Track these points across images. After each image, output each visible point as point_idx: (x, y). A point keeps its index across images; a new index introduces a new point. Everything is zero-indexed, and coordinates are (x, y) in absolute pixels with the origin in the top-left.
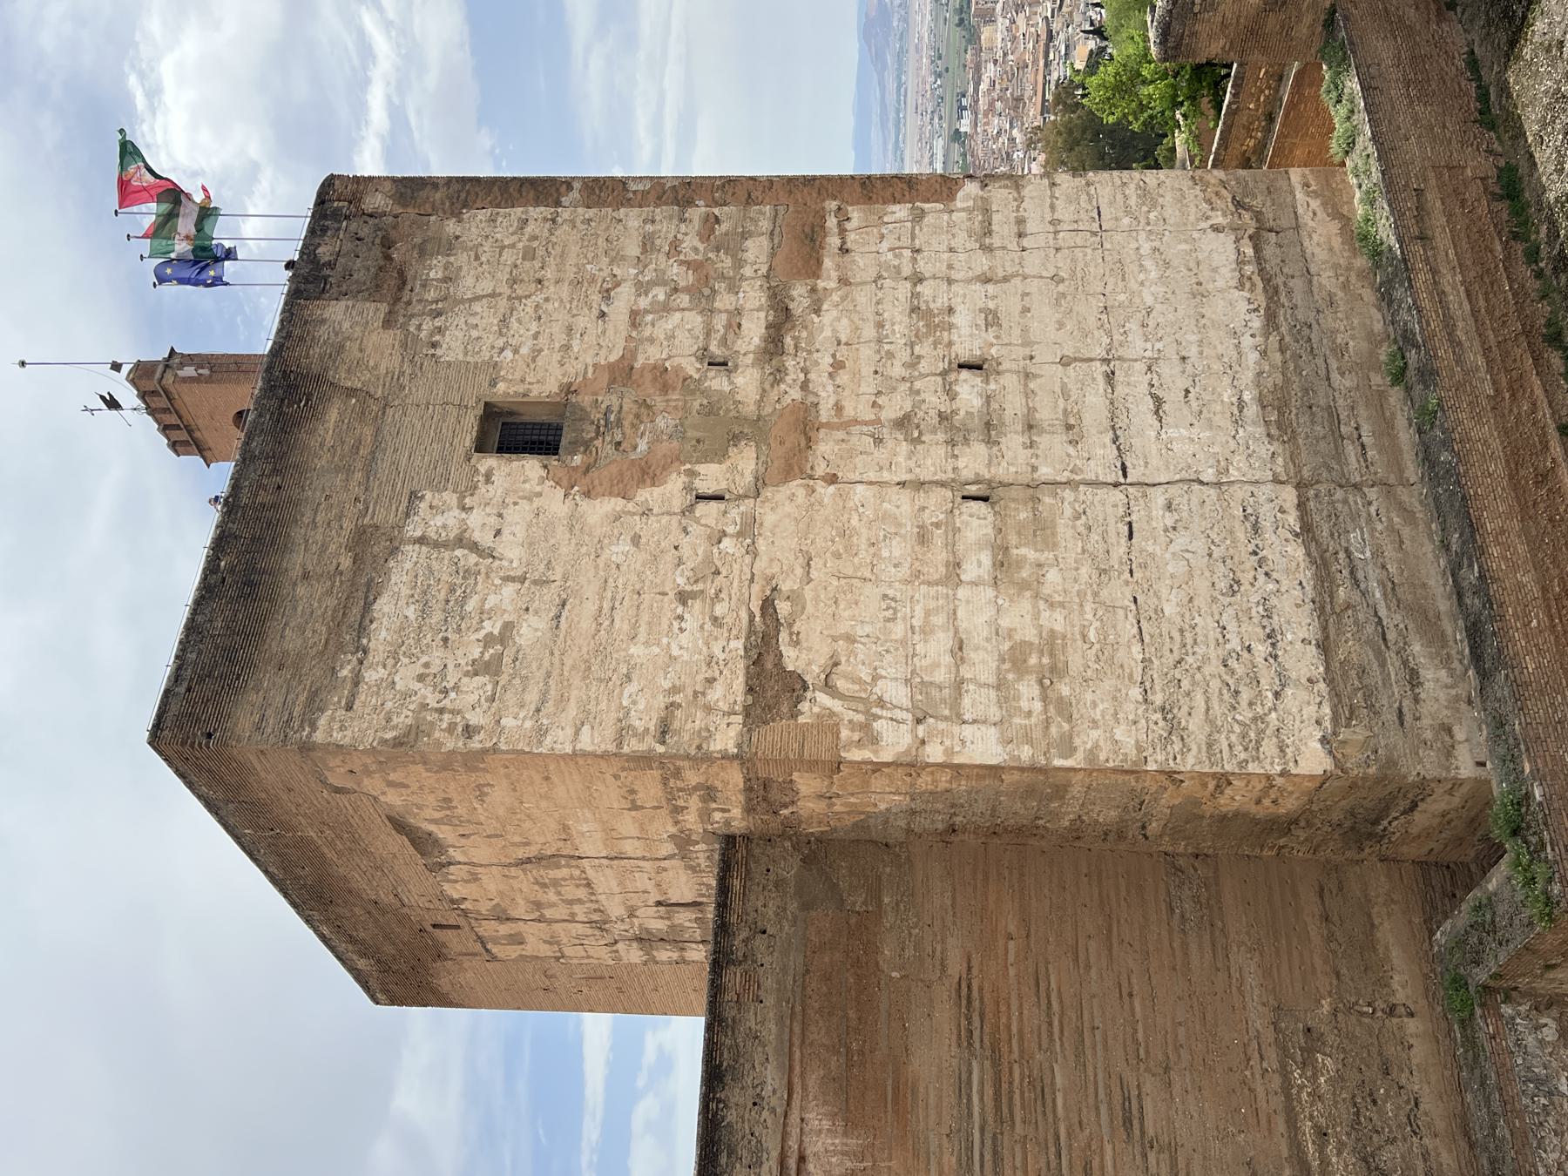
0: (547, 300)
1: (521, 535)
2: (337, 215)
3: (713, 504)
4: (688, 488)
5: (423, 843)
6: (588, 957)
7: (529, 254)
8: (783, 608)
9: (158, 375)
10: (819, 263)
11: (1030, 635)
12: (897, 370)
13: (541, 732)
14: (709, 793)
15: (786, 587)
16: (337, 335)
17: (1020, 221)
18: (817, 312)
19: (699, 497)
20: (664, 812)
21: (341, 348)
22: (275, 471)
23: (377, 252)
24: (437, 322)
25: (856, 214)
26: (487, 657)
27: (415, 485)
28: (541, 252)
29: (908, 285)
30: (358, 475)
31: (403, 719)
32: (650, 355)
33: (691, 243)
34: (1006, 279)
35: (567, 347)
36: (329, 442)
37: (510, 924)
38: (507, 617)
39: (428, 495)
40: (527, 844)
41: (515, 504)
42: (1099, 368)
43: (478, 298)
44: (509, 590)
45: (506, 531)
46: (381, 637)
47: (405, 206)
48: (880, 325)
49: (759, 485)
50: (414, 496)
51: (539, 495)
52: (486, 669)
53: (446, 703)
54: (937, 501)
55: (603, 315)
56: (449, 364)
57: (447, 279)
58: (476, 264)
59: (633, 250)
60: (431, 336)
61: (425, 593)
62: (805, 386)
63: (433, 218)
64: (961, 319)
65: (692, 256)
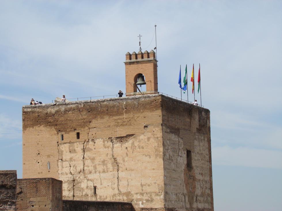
5: (121, 139)
6: (63, 167)
19: (185, 196)
20: (141, 191)
37: (81, 151)
40: (124, 161)
49: (187, 209)
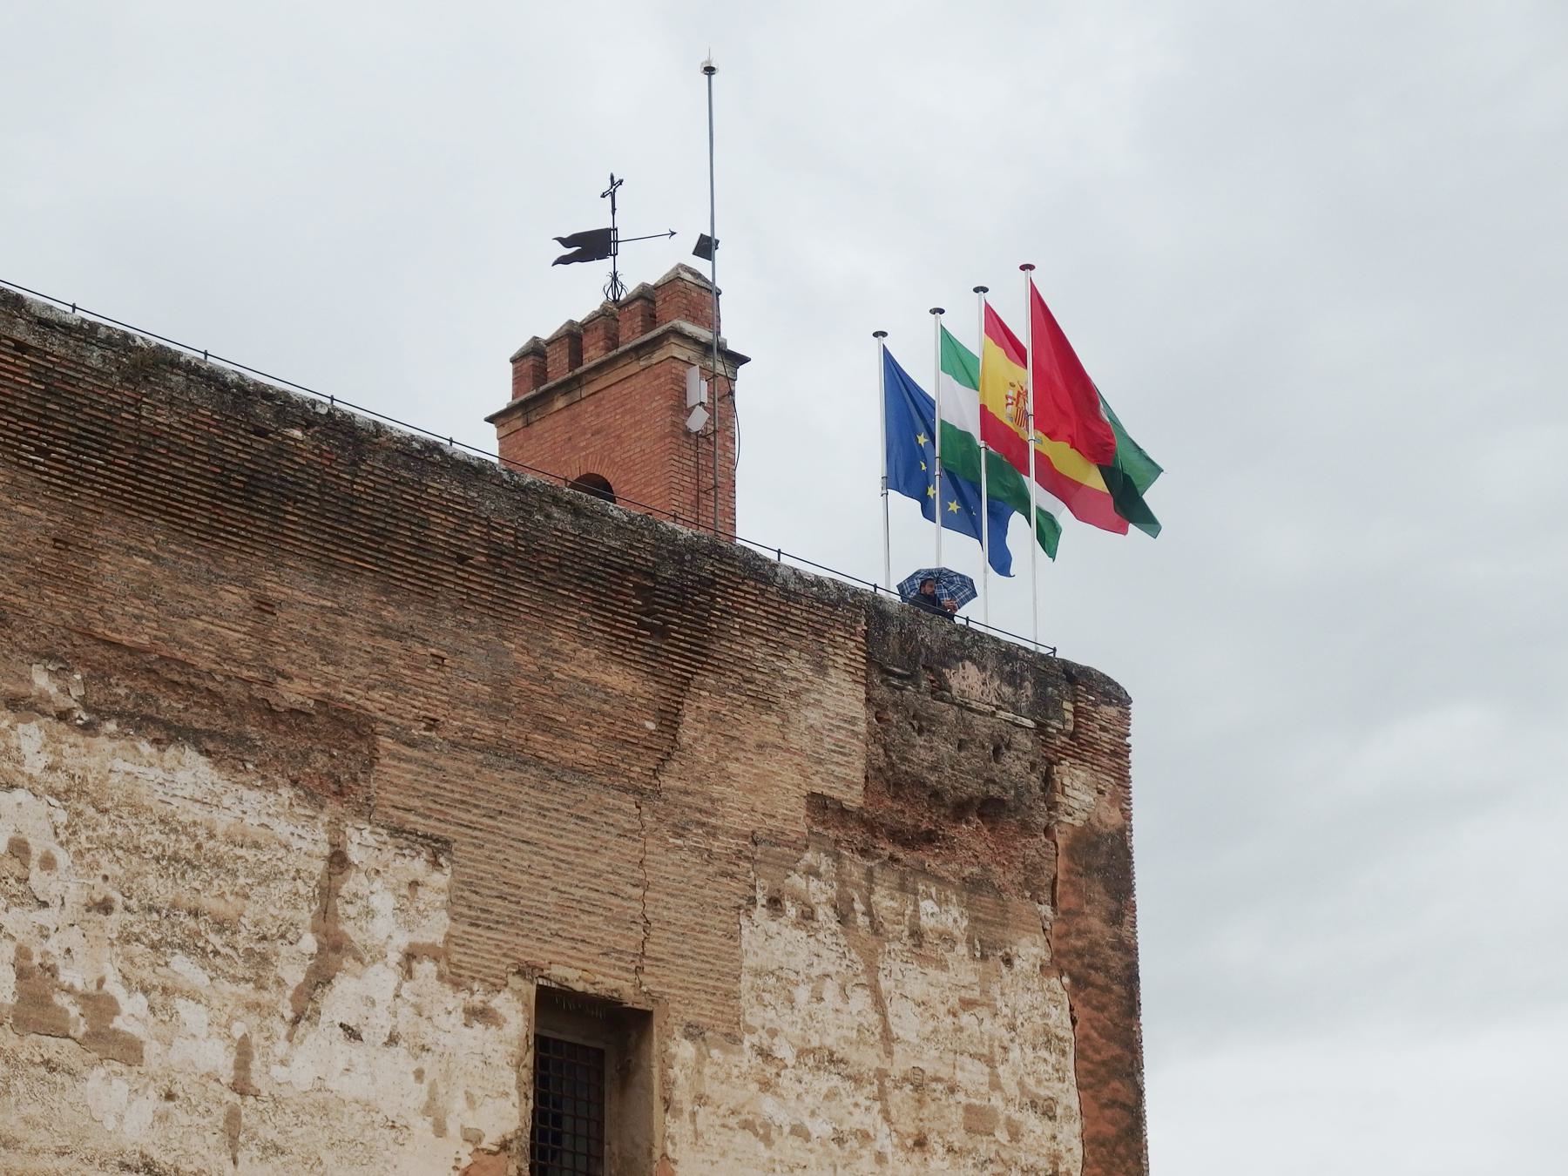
0: (880, 1158)
1: (351, 1087)
2: (1043, 707)
7: (978, 1120)
9: (689, 328)
16: (794, 695)
21: (765, 703)
22: (497, 555)
23: (974, 787)
24: (824, 914)
26: (62, 1000)
27: (462, 850)
28: (985, 1148)
30: (487, 729)
36: (563, 671)
38: (152, 1049)
39: (440, 879)
41: (419, 1074)
43: (879, 1002)
44: (219, 1058)
45: (354, 1051)
47: (1071, 851)
50: (437, 849)
51: (440, 1130)
56: (733, 936)
57: (917, 934)
58: (954, 1001)
60: (795, 899)
61: (218, 863)
63: (1046, 910)
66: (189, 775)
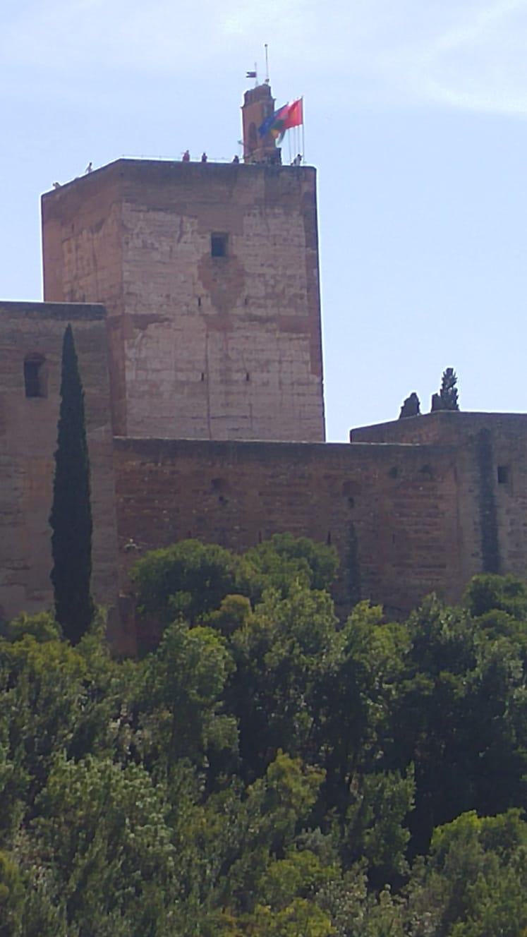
3: (197, 303)
4: (203, 295)
5: (99, 226)
7: (285, 240)
8: (166, 323)
10: (286, 331)
11: (162, 389)
12: (245, 356)
13: (127, 262)
14: (115, 307)
15: (173, 324)
17: (304, 395)
18: (267, 331)
25: (306, 343)
29: (277, 358)
31: (129, 226)
32: (249, 281)
33: (292, 291)
34: (280, 389)
35: (250, 255)
42: (248, 414)
44: (168, 249)
46: (152, 215)
48: (263, 350)
49: (205, 316)
50: (196, 217)
52: (145, 246)
53: (134, 236)
54: (203, 367)
55: (262, 265)
59: (288, 272)
62: (238, 328)
64: (265, 375)
65: (286, 292)
66: (160, 216)
